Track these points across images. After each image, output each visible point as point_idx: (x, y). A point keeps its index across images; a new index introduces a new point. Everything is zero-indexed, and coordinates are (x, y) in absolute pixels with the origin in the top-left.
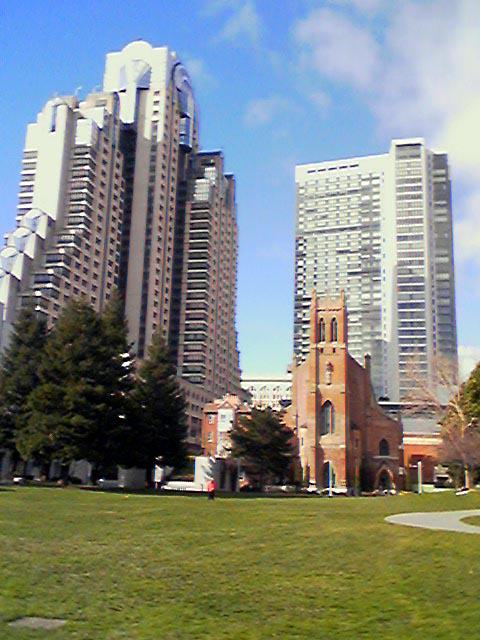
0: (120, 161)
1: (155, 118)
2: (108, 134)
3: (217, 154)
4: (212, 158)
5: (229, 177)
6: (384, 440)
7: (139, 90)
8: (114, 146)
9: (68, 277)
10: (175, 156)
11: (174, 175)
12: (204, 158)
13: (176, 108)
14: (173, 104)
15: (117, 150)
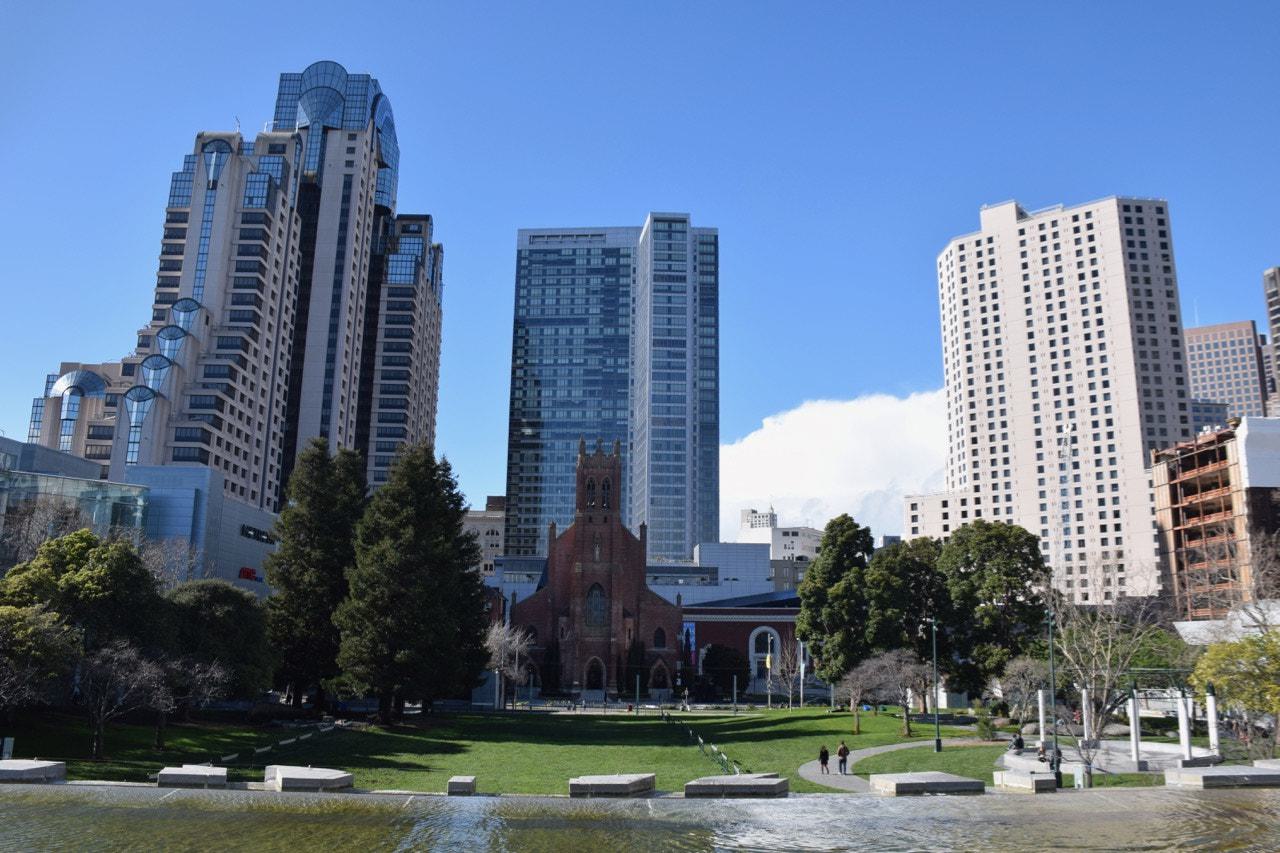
0: (297, 228)
1: (349, 171)
2: (286, 194)
3: (427, 218)
4: (419, 224)
5: (438, 249)
6: (659, 629)
7: (326, 130)
8: (292, 209)
9: (233, 398)
10: (370, 221)
11: (367, 248)
12: (404, 223)
13: (374, 155)
14: (372, 150)
15: (295, 213)
